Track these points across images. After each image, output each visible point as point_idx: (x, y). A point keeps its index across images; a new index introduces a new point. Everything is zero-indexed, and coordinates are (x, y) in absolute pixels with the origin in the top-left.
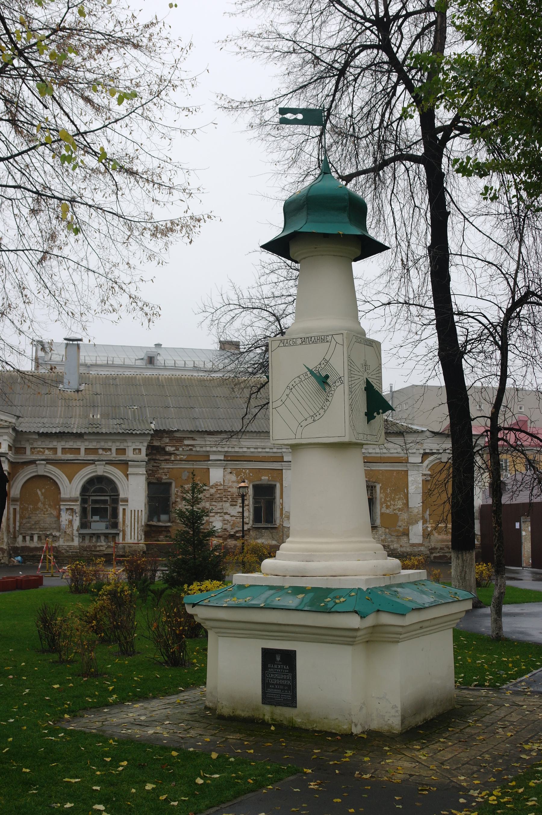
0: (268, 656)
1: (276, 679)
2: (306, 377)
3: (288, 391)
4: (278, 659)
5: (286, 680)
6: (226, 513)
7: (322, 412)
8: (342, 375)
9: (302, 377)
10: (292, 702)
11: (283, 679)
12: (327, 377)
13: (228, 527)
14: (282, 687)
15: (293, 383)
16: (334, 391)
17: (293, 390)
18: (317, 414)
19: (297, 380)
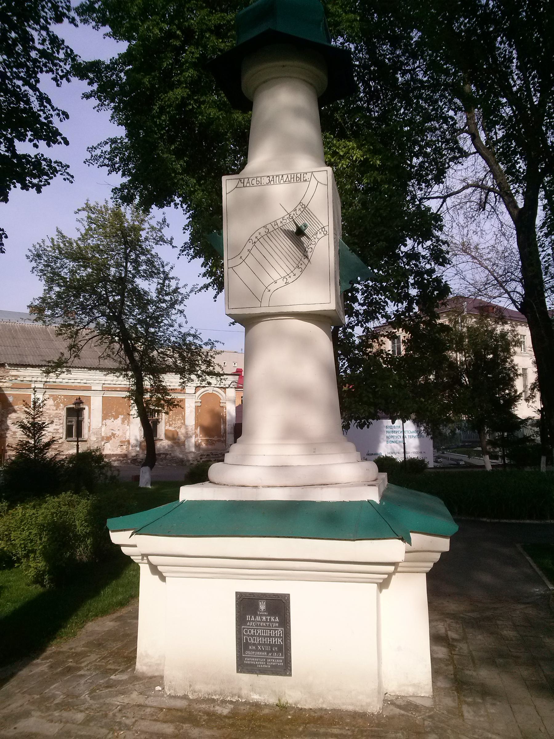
1: (259, 636)
4: (262, 606)
5: (275, 637)
8: (325, 224)
9: (269, 226)
10: (285, 669)
11: (270, 637)
14: (268, 648)
15: (257, 234)
16: (315, 244)
17: (258, 244)
18: (292, 275)
19: (263, 231)
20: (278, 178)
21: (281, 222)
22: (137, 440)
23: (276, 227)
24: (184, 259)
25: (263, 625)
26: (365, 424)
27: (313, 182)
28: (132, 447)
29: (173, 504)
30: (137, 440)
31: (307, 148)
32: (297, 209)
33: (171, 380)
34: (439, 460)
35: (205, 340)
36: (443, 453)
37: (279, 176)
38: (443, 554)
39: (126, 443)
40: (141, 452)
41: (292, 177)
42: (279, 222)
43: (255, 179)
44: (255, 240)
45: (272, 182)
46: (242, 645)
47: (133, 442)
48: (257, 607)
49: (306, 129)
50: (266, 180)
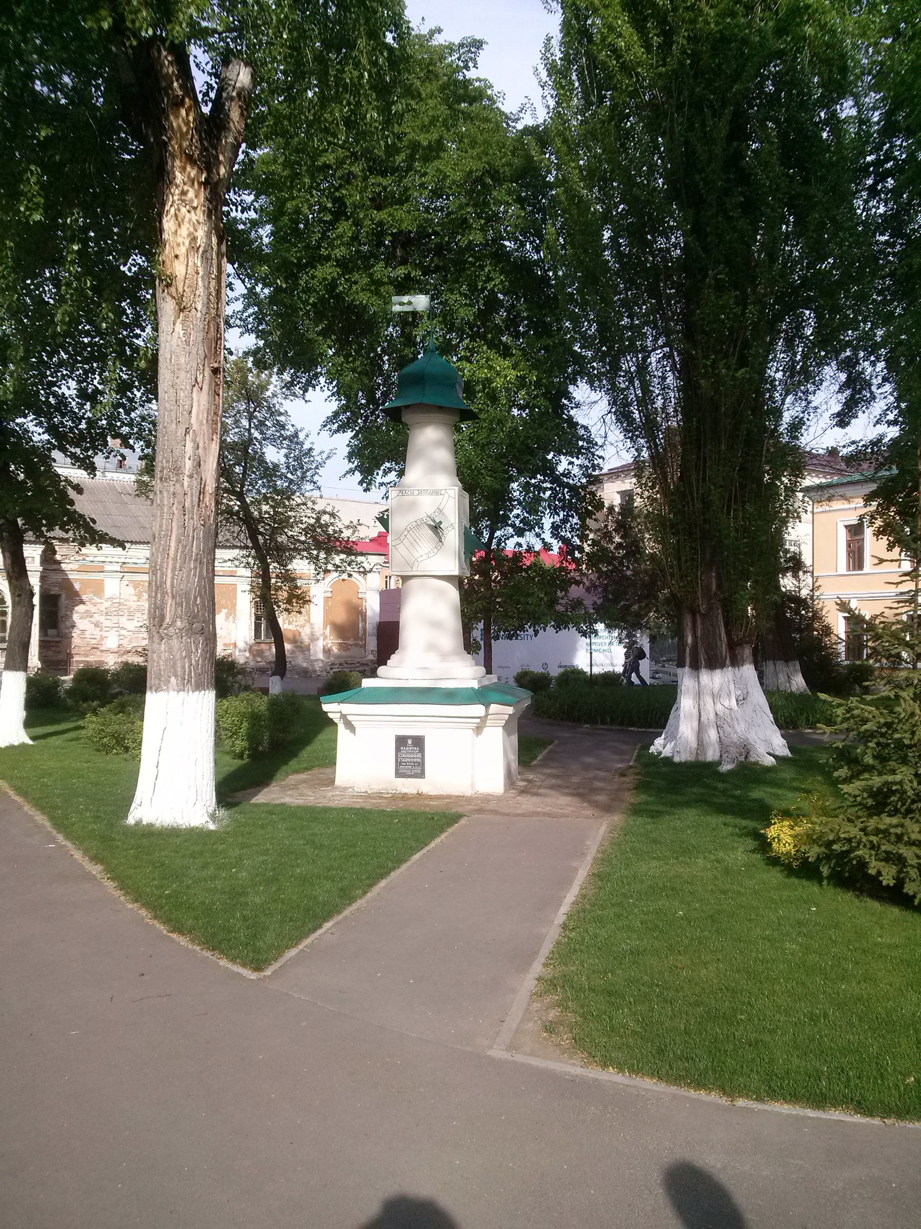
0: (401, 741)
3: (406, 533)
4: (410, 742)
6: (123, 628)
10: (421, 775)
12: (441, 522)
13: (125, 643)
19: (414, 524)
22: (246, 643)
24: (325, 434)
25: (410, 752)
26: (513, 635)
27: (446, 496)
28: (240, 651)
29: (358, 689)
30: (246, 643)
31: (444, 469)
33: (300, 566)
34: (657, 676)
35: (347, 523)
36: (663, 666)
38: (510, 715)
39: (231, 647)
40: (251, 658)
46: (398, 763)
47: (241, 645)
48: (407, 743)
49: (444, 456)
50: (416, 492)
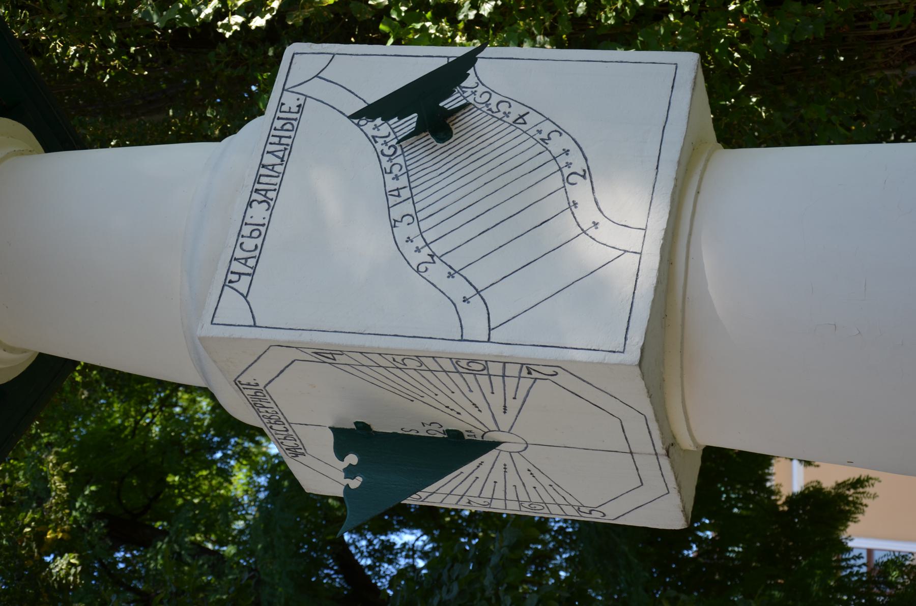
2: (405, 193)
3: (437, 272)
7: (557, 144)
9: (396, 213)
17: (438, 248)
18: (562, 161)
20: (263, 179)
21: (396, 178)
23: (405, 193)
27: (315, 88)
32: (371, 133)
37: (259, 176)
41: (276, 140)
42: (392, 185)
43: (241, 240)
44: (424, 255)
45: (271, 195)
